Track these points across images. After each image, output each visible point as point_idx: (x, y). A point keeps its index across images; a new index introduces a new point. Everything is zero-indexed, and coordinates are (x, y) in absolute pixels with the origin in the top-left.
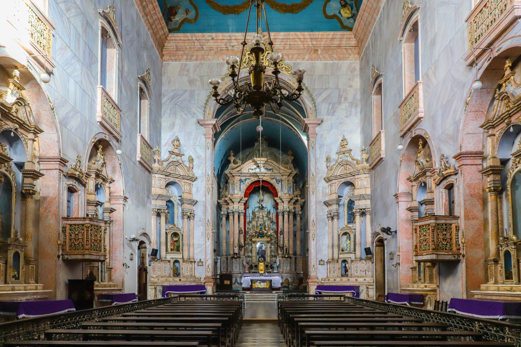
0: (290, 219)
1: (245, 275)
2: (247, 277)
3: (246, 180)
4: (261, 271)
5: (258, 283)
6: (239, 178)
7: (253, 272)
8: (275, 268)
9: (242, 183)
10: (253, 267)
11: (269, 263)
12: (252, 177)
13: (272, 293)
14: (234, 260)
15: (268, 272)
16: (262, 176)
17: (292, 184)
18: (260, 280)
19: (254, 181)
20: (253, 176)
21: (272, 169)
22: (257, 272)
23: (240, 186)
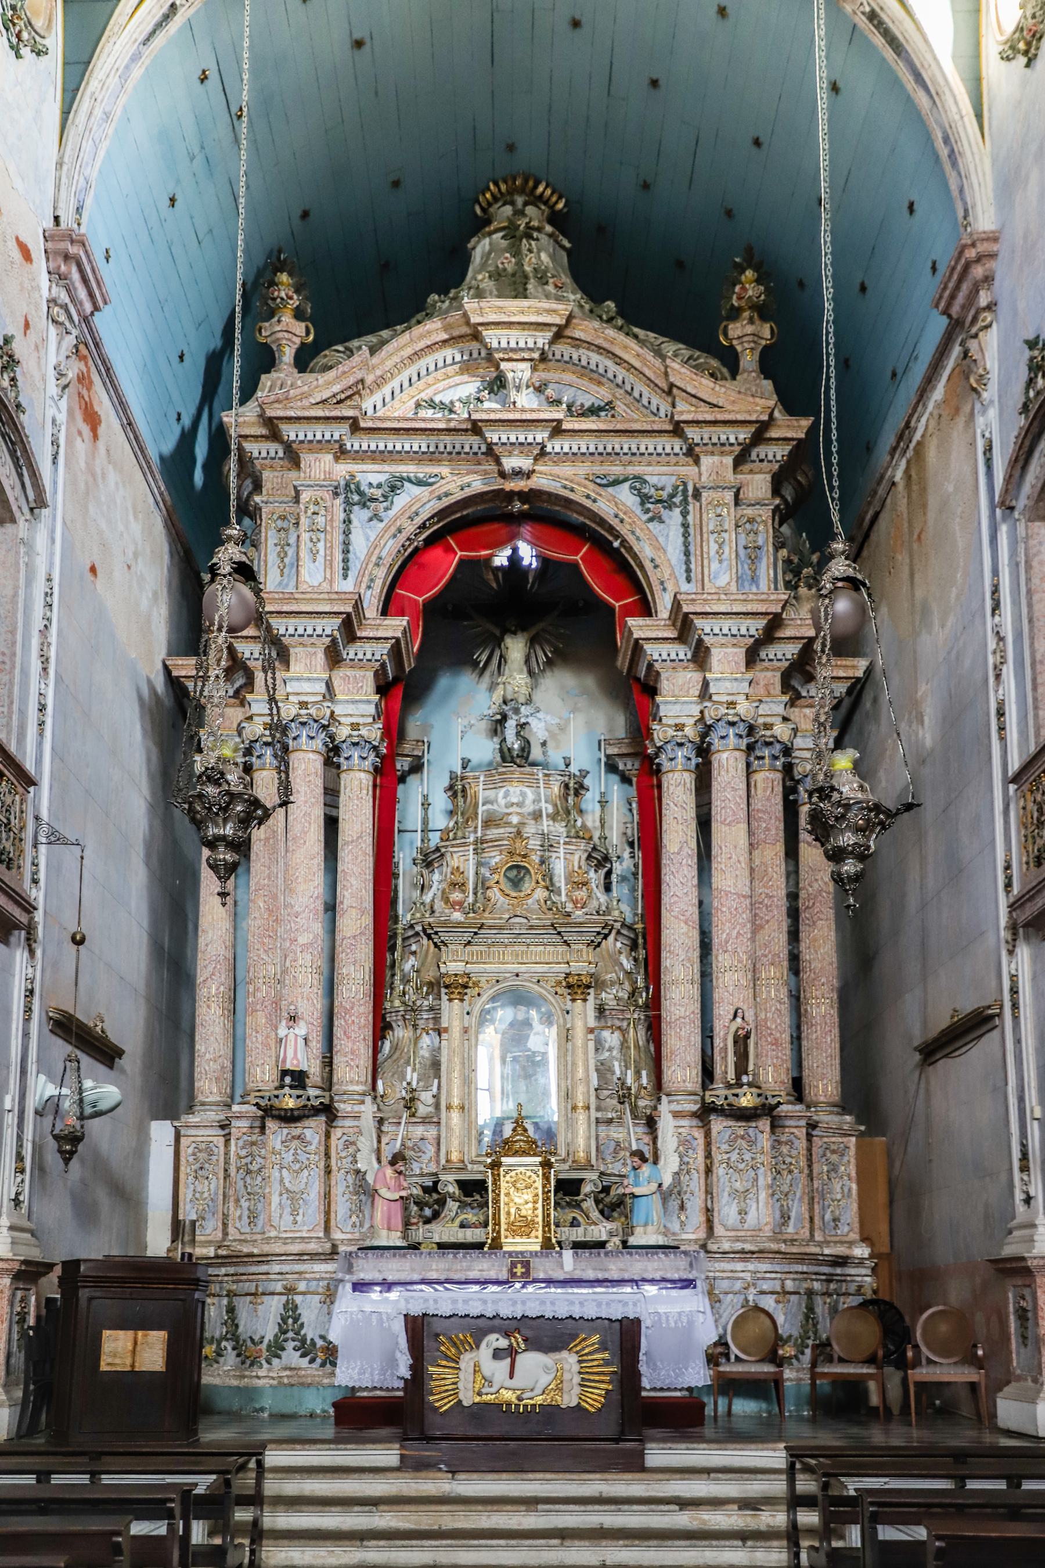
0: (757, 804)
1: (368, 1269)
2: (388, 1286)
3: (394, 487)
4: (515, 1230)
5: (485, 1353)
6: (342, 470)
7: (441, 1246)
8: (641, 1205)
9: (359, 516)
10: (442, 1202)
11: (589, 1166)
12: (445, 470)
13: (635, 1464)
14: (277, 1134)
15: (577, 1246)
16: (522, 446)
17: (765, 536)
18: (509, 1326)
19: (459, 496)
20: (455, 456)
21: (609, 406)
22: (479, 1246)
23: (347, 533)
